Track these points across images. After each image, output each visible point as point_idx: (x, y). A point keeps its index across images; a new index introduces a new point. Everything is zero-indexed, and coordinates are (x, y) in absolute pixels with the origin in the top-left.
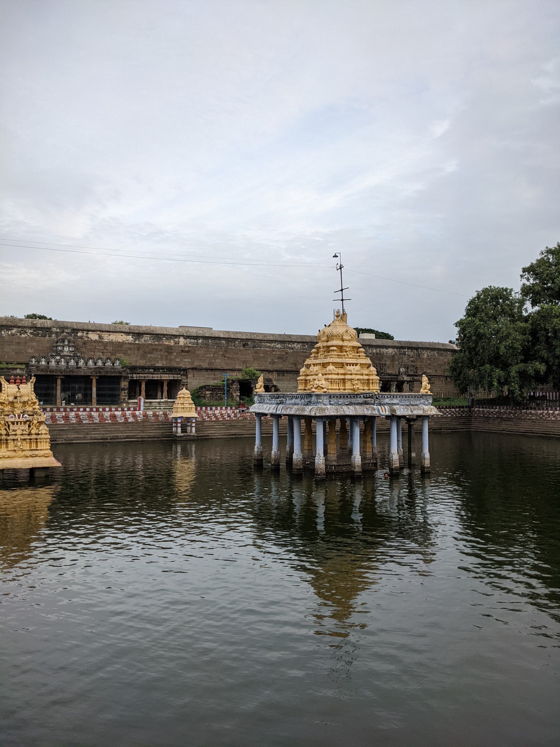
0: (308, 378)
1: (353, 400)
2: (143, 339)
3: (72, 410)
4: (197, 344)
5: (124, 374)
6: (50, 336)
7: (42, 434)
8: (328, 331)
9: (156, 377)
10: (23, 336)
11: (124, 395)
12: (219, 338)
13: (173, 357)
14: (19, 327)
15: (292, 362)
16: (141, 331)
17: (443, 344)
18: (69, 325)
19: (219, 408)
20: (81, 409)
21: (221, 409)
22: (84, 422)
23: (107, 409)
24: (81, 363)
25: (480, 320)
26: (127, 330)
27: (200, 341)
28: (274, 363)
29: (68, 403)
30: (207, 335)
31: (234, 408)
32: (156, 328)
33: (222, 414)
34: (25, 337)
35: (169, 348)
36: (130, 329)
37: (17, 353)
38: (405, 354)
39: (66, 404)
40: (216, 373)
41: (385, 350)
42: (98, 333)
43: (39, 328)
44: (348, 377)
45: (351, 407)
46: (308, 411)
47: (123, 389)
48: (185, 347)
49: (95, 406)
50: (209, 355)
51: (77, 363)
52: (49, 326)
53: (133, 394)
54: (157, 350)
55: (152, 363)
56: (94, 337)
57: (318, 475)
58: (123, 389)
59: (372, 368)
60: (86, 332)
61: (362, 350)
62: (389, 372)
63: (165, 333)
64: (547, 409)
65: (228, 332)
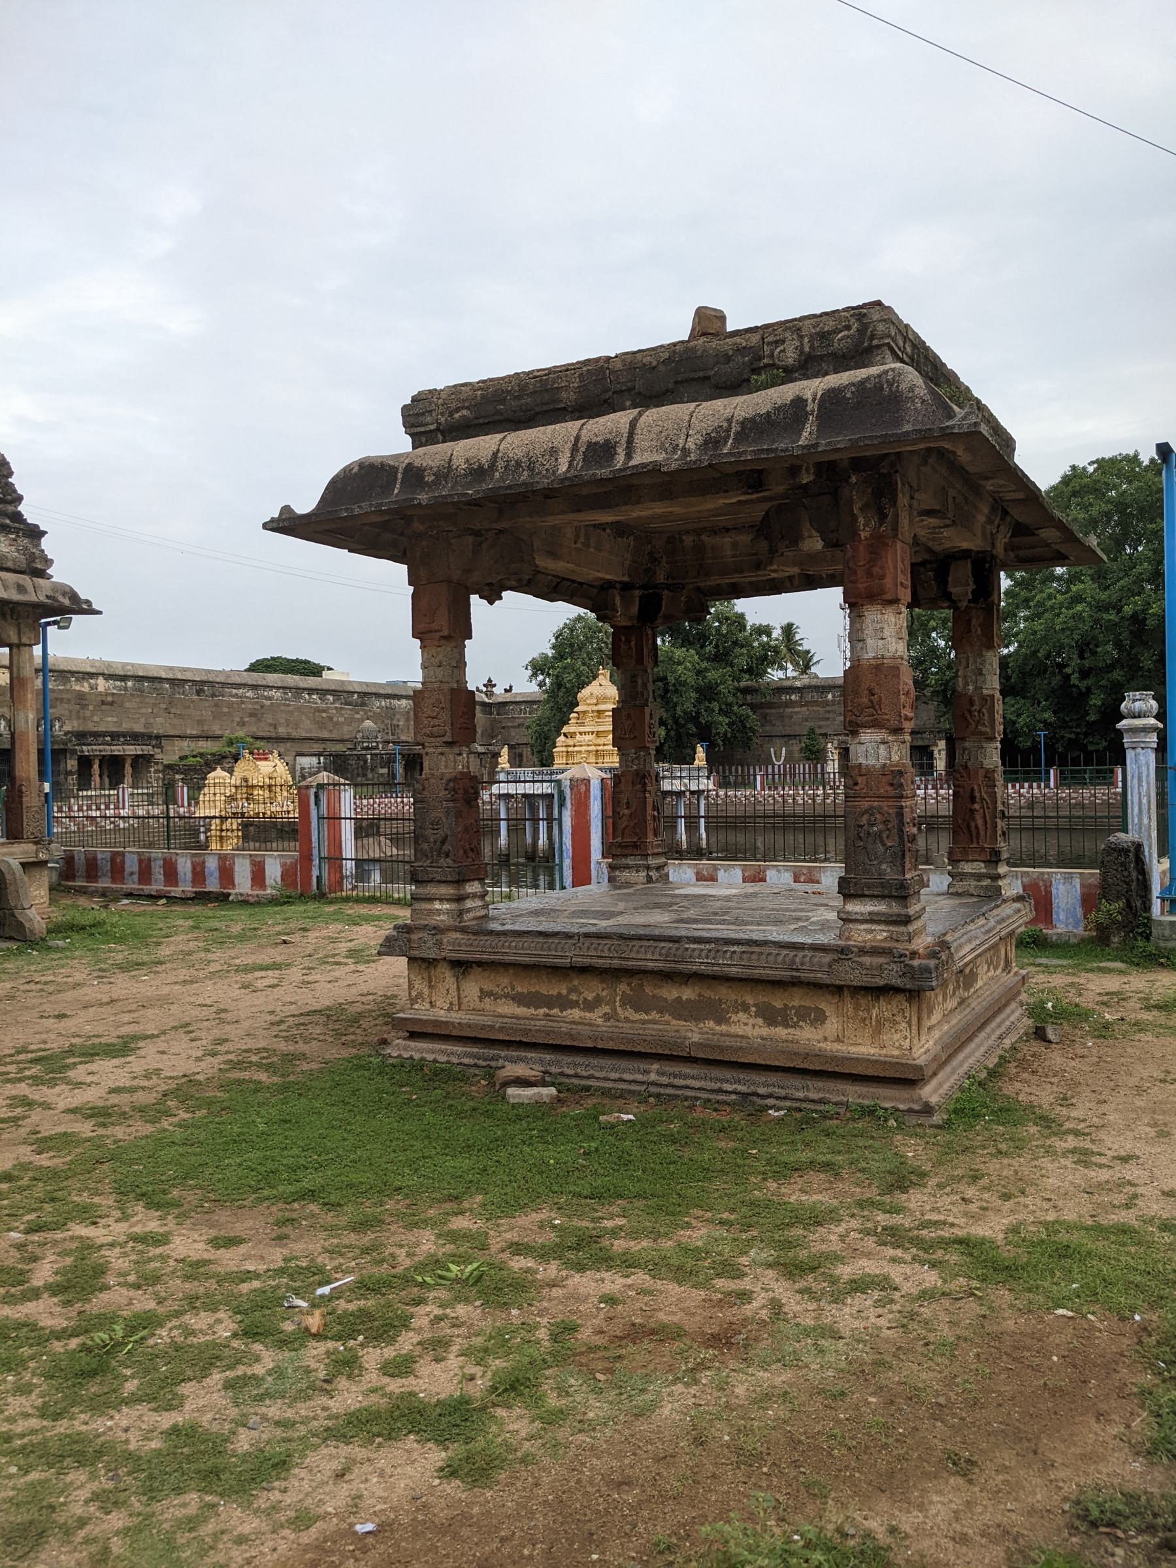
4: (126, 689)
9: (117, 750)
12: (160, 680)
13: (88, 713)
15: (270, 721)
27: (130, 684)
30: (141, 674)
35: (81, 696)
41: (396, 702)
48: (107, 694)
50: (144, 710)
65: (171, 669)
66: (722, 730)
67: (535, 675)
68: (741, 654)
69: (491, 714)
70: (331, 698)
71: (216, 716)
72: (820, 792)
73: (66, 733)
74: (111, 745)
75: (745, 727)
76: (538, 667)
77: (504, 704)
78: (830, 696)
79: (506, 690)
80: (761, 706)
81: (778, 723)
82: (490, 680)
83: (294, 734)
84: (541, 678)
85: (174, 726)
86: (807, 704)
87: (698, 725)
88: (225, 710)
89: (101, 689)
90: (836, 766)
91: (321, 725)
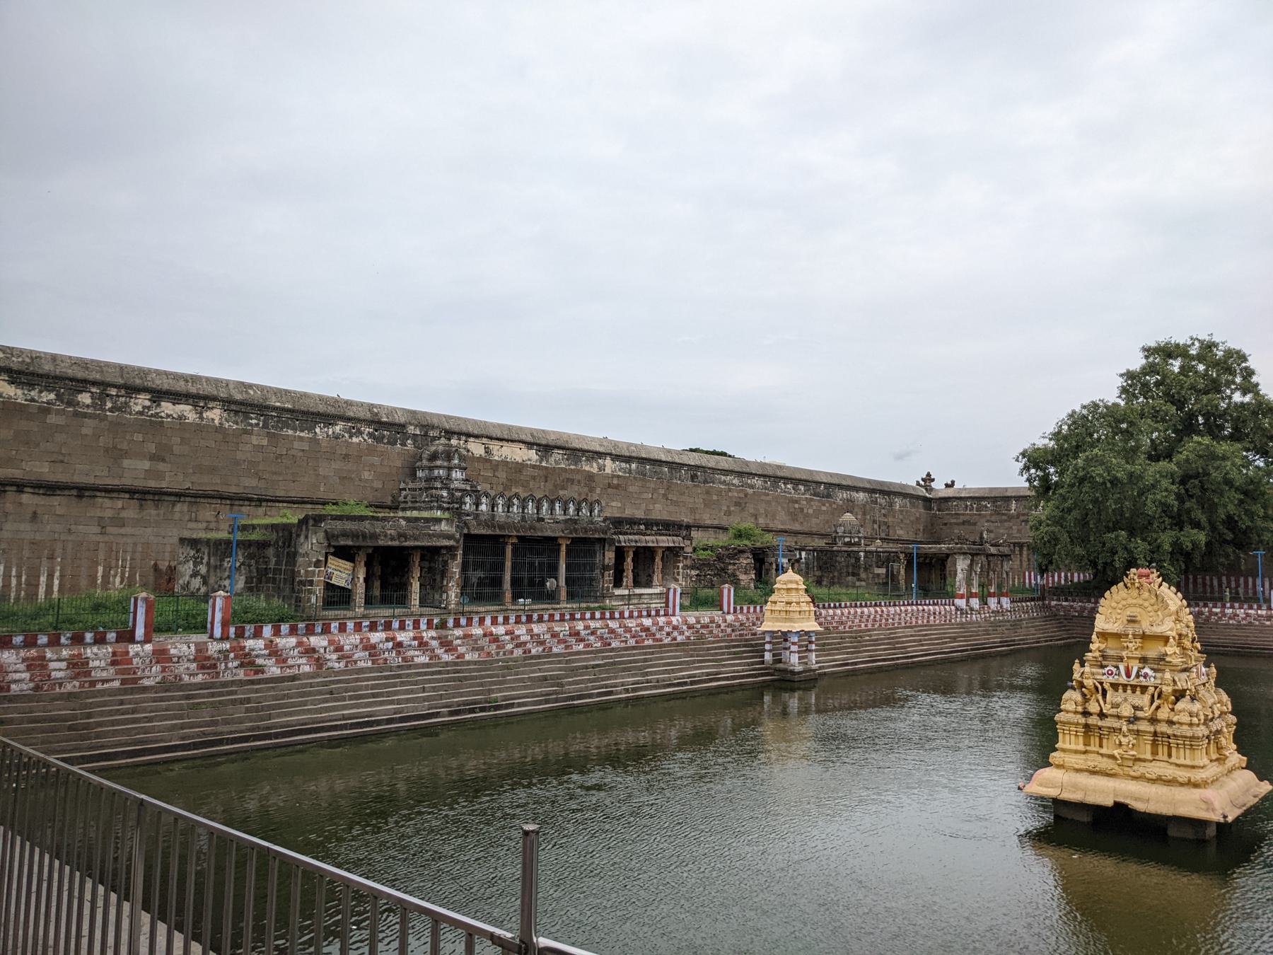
4: (630, 472)
9: (650, 540)
10: (355, 440)
12: (659, 462)
14: (349, 419)
16: (551, 439)
18: (435, 422)
22: (613, 645)
26: (529, 439)
27: (634, 466)
28: (728, 513)
32: (569, 435)
34: (359, 444)
37: (342, 479)
38: (876, 503)
41: (854, 494)
42: (485, 441)
43: (386, 423)
48: (613, 476)
50: (645, 496)
52: (402, 420)
56: (476, 448)
58: (605, 568)
60: (464, 438)
65: (669, 451)
67: (1027, 468)
69: (930, 509)
70: (802, 488)
71: (707, 504)
73: (606, 519)
74: (645, 534)
76: (1034, 459)
77: (946, 499)
79: (947, 485)
82: (929, 475)
83: (771, 525)
84: (1033, 471)
88: (715, 497)
89: (608, 471)
91: (793, 516)
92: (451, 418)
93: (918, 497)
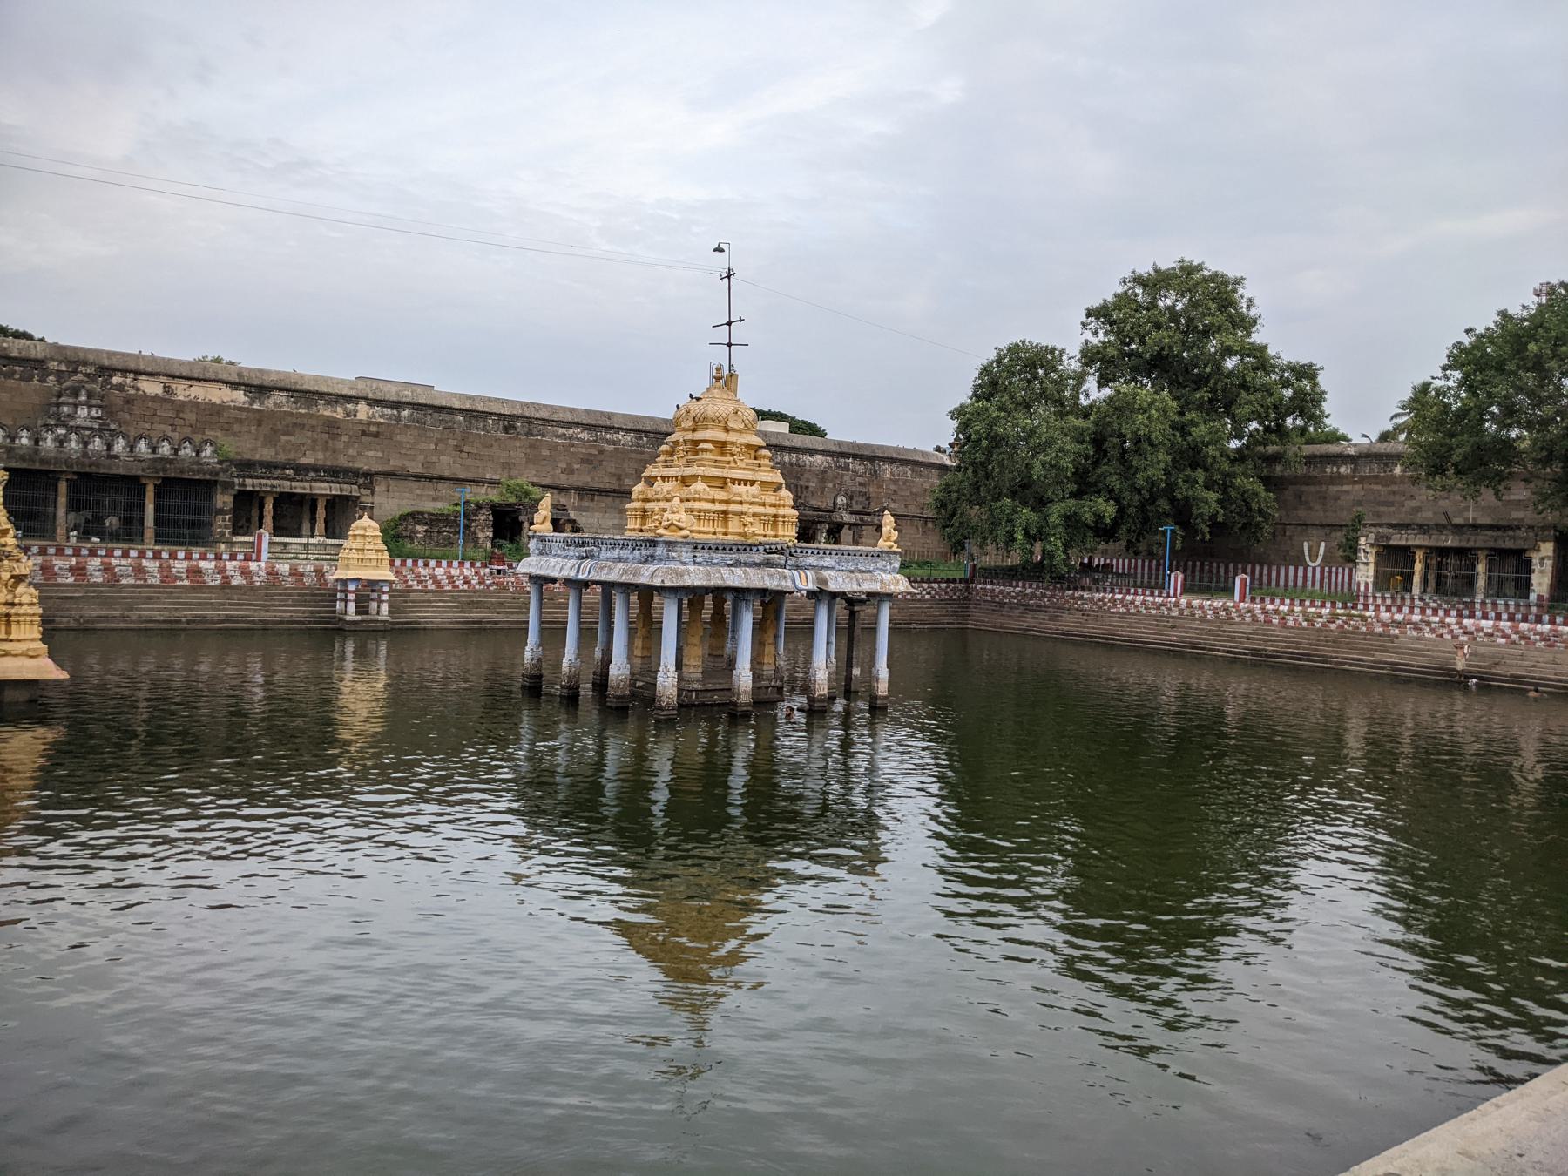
0: (649, 506)
1: (743, 557)
2: (271, 401)
3: (93, 553)
4: (398, 418)
5: (222, 477)
6: (42, 380)
7: (21, 604)
8: (696, 408)
9: (300, 487)
11: (222, 524)
12: (451, 410)
13: (340, 445)
16: (267, 381)
17: (923, 454)
18: (91, 358)
19: (444, 563)
20: (118, 553)
21: (450, 565)
22: (124, 581)
23: (181, 555)
24: (120, 446)
25: (1000, 409)
26: (234, 378)
27: (405, 413)
29: (85, 535)
30: (422, 401)
31: (478, 564)
32: (302, 377)
33: (450, 577)
35: (332, 426)
36: (240, 375)
38: (847, 468)
39: (79, 539)
40: (440, 486)
41: (807, 458)
42: (163, 379)
43: (15, 358)
44: (733, 508)
45: (737, 571)
46: (649, 575)
47: (221, 511)
48: (369, 424)
49: (150, 546)
50: (423, 446)
51: (109, 446)
52: (40, 356)
53: (242, 525)
54: (302, 426)
55: (292, 456)
56: (151, 387)
57: (661, 709)
58: (221, 511)
59: (785, 492)
61: (766, 452)
62: (814, 503)
63: (325, 390)
64: (1112, 591)
66: (1206, 510)
68: (1250, 402)
72: (1325, 611)
75: (1250, 509)
78: (1398, 470)
80: (1296, 480)
81: (1317, 507)
85: (467, 468)
86: (1362, 480)
87: (1173, 500)
90: (1371, 572)
92: (115, 354)
93: (929, 465)
